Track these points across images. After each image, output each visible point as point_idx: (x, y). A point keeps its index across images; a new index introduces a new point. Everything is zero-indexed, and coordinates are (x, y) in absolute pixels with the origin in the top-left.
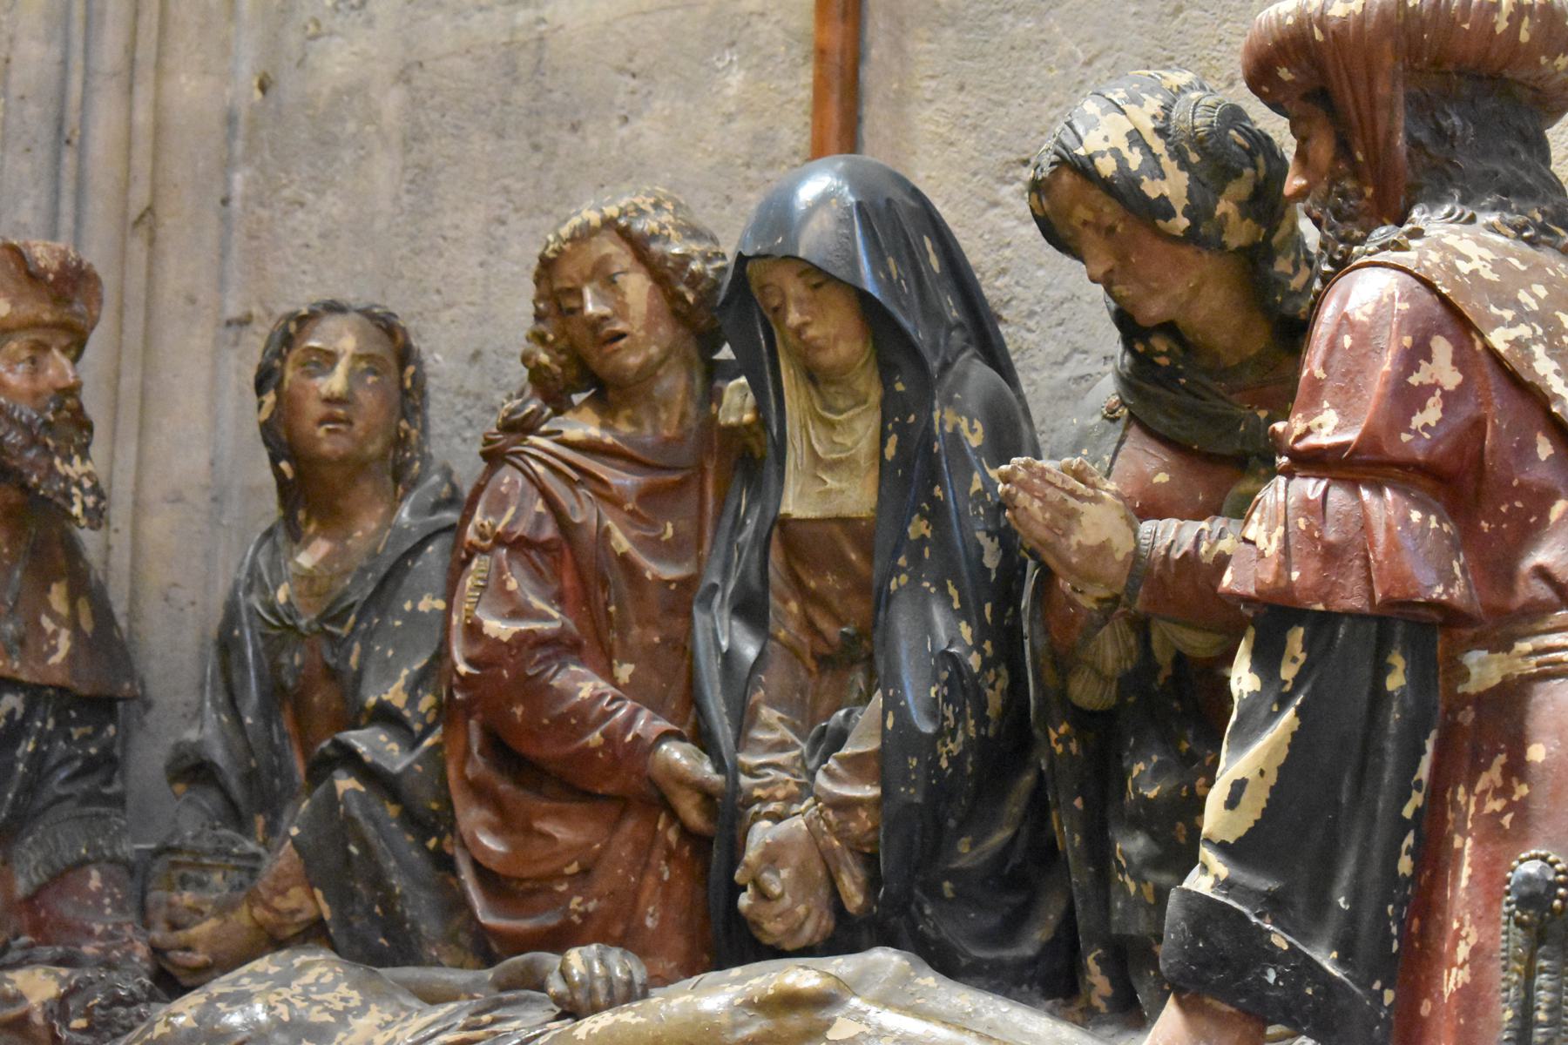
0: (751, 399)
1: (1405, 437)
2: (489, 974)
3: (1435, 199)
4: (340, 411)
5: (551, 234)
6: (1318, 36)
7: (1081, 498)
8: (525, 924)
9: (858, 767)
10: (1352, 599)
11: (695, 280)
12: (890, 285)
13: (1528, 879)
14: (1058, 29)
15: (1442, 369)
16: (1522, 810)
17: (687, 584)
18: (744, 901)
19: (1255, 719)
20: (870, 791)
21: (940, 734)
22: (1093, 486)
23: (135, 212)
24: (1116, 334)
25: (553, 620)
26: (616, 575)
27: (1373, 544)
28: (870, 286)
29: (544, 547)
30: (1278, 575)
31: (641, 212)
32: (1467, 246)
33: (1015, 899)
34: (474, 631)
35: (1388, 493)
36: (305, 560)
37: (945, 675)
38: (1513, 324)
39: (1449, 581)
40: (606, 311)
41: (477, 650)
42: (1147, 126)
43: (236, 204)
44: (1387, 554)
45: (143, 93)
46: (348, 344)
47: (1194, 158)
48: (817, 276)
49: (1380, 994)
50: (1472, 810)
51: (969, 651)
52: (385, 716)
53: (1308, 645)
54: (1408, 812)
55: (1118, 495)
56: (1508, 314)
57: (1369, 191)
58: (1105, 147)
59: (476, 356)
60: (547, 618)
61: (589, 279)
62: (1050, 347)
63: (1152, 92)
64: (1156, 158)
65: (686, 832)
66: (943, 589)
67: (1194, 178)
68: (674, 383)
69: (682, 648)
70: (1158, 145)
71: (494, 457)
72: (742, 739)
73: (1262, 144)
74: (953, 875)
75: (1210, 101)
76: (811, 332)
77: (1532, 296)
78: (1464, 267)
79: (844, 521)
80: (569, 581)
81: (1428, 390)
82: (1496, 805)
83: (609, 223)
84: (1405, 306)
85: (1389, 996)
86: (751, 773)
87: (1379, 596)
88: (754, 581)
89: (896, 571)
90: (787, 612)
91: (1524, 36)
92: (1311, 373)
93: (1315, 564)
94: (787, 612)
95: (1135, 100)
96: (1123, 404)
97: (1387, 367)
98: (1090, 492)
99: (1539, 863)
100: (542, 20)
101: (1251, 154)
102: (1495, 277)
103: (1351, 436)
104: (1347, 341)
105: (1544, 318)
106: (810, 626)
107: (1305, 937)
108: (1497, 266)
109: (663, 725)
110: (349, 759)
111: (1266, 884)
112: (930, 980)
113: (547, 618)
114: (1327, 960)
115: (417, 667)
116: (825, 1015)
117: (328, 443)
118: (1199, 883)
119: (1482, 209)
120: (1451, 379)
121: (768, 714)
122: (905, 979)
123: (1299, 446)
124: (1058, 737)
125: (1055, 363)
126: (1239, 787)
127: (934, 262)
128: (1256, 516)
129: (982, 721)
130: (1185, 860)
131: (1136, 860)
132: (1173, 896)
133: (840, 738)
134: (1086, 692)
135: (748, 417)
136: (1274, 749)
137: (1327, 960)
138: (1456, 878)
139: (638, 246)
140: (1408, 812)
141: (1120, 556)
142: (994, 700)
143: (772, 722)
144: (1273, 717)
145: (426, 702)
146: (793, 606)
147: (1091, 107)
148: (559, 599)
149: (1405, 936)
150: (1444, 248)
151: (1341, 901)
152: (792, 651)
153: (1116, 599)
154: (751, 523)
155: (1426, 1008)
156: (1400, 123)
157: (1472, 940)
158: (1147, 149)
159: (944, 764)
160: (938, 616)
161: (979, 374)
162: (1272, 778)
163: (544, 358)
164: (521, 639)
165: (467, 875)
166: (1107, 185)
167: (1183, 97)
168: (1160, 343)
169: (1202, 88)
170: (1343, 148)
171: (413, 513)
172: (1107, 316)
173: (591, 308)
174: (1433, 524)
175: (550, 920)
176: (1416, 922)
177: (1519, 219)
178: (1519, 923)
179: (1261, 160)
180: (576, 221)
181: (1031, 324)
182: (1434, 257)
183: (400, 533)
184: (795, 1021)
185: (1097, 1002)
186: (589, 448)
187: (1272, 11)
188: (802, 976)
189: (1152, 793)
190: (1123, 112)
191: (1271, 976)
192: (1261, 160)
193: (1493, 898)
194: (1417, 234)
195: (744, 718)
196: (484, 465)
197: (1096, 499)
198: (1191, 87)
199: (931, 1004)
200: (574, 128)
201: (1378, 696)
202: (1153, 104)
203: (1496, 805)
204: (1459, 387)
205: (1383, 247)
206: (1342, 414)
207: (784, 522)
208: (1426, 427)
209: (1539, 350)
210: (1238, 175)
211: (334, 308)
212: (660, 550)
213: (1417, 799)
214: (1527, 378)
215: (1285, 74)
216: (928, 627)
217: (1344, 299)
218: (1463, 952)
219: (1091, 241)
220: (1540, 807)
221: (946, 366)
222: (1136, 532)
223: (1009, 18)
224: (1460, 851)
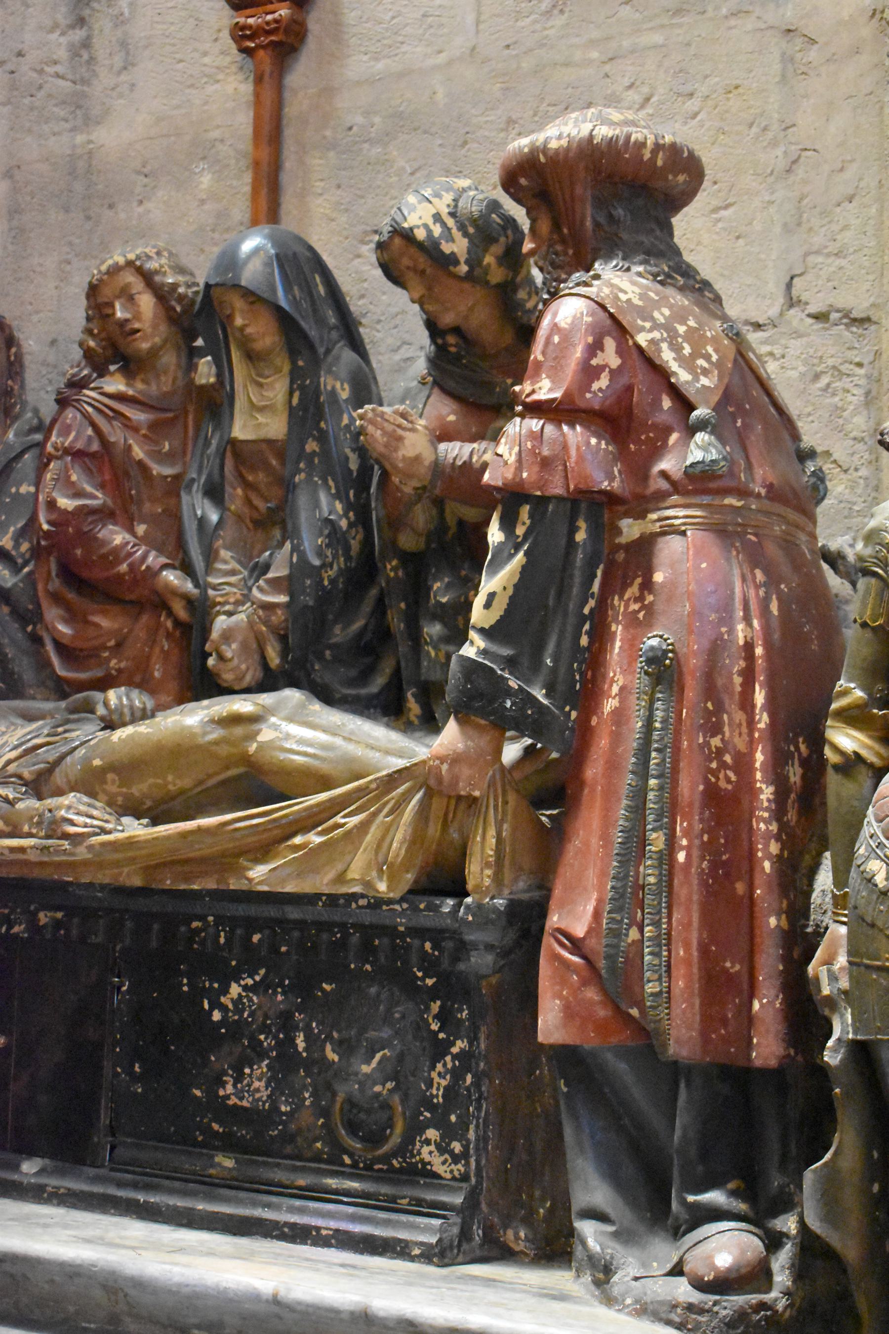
0: (214, 370)
1: (588, 395)
2: (63, 704)
3: (608, 257)
5: (95, 269)
6: (542, 159)
7: (404, 429)
8: (83, 676)
9: (276, 585)
10: (557, 490)
11: (181, 298)
12: (295, 302)
13: (652, 648)
14: (395, 153)
15: (610, 356)
16: (649, 610)
17: (177, 478)
18: (211, 662)
19: (502, 556)
20: (283, 599)
21: (323, 566)
22: (411, 422)
24: (426, 333)
25: (98, 498)
26: (134, 472)
27: (569, 458)
28: (283, 303)
29: (93, 456)
30: (515, 475)
31: (149, 258)
32: (625, 284)
33: (367, 660)
34: (51, 504)
35: (578, 428)
37: (326, 532)
38: (650, 330)
39: (612, 479)
40: (128, 316)
41: (53, 517)
42: (444, 211)
44: (577, 463)
47: (471, 230)
48: (250, 296)
49: (569, 713)
50: (622, 609)
51: (340, 517)
53: (531, 516)
54: (586, 611)
55: (426, 427)
56: (648, 325)
57: (571, 252)
58: (419, 223)
59: (53, 342)
60: (93, 497)
61: (118, 297)
62: (390, 341)
63: (447, 191)
64: (449, 229)
65: (177, 623)
66: (325, 482)
67: (471, 241)
68: (169, 359)
69: (175, 516)
70: (450, 222)
71: (63, 402)
72: (209, 569)
73: (510, 222)
74: (331, 647)
75: (481, 197)
76: (249, 330)
77: (661, 315)
78: (623, 297)
79: (269, 442)
80: (107, 477)
81: (601, 368)
82: (636, 607)
83: (130, 264)
84: (589, 319)
85: (574, 714)
86: (214, 588)
87: (572, 487)
88: (216, 476)
89: (299, 471)
90: (235, 495)
91: (660, 163)
92: (535, 358)
93: (536, 469)
94: (235, 495)
95: (438, 195)
96: (430, 374)
97: (578, 355)
98: (410, 426)
99: (658, 639)
100: (90, 142)
101: (504, 228)
102: (640, 303)
103: (558, 394)
104: (556, 339)
105: (668, 328)
106: (248, 502)
107: (528, 682)
108: (642, 296)
109: (163, 560)
111: (506, 652)
112: (317, 706)
113: (93, 497)
114: (539, 694)
115: (19, 525)
116: (256, 727)
118: (469, 651)
119: (635, 264)
120: (615, 362)
122: (303, 706)
123: (528, 400)
124: (391, 568)
125: (393, 351)
126: (492, 596)
127: (322, 290)
128: (503, 440)
129: (348, 558)
130: (461, 638)
131: (435, 638)
132: (454, 658)
133: (266, 568)
134: (407, 541)
135: (212, 380)
136: (512, 574)
137: (539, 694)
138: (613, 647)
139: (147, 278)
140: (586, 611)
141: (427, 463)
142: (355, 545)
144: (511, 556)
145: (25, 547)
146: (239, 491)
147: (412, 199)
148: (102, 486)
149: (583, 682)
150: (612, 285)
151: (548, 661)
152: (239, 518)
153: (424, 488)
154: (214, 443)
155: (594, 721)
156: (589, 211)
157: (620, 683)
158: (444, 224)
159: (326, 583)
160: (323, 498)
161: (348, 356)
162: (510, 591)
163: (92, 343)
164: (79, 509)
165: (50, 648)
166: (420, 245)
167: (465, 195)
168: (451, 339)
169: (477, 189)
170: (556, 226)
171: (16, 435)
172: (421, 323)
173: (119, 314)
174: (603, 446)
175: (99, 673)
176: (590, 673)
177: (655, 270)
178: (646, 673)
179: (509, 232)
180: (110, 262)
181: (379, 327)
182: (606, 291)
183: (8, 446)
184: (239, 731)
185: (413, 718)
186: (120, 397)
187: (516, 144)
188: (243, 705)
189: (444, 600)
190: (430, 202)
191: (508, 704)
192: (509, 232)
193: (632, 660)
194: (597, 277)
195: (210, 556)
196: (56, 407)
197: (413, 430)
198: (470, 188)
199: (317, 721)
200: (111, 206)
201: (571, 544)
202: (448, 198)
203: (636, 607)
204: (619, 367)
205: (578, 285)
206: (553, 382)
207: (234, 443)
208: (600, 390)
209: (664, 346)
210: (495, 240)
212: (163, 458)
213: (592, 603)
214: (658, 362)
215: (523, 181)
216: (317, 505)
217: (555, 315)
218: (615, 689)
219: (412, 279)
220: (659, 607)
221: (328, 351)
222: (436, 449)
223: (366, 146)
224: (615, 633)
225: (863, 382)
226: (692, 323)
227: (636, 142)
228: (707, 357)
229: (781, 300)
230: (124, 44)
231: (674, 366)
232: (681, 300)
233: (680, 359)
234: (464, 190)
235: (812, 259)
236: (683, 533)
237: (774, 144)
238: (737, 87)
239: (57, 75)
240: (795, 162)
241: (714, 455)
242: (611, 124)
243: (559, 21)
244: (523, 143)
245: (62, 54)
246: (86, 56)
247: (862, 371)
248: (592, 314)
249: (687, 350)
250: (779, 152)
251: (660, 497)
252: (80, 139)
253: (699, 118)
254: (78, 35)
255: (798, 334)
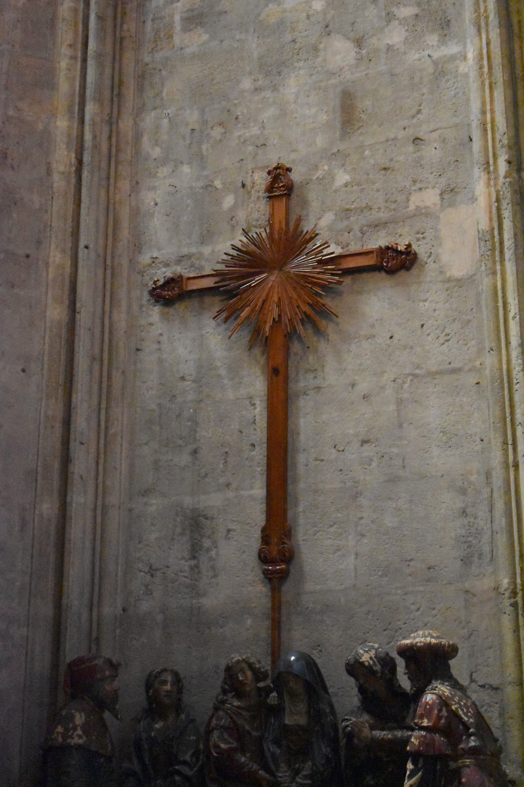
4: (170, 694)
9: (306, 777)
11: (262, 672)
15: (444, 713)
23: (93, 639)
25: (235, 745)
32: (445, 690)
34: (217, 746)
36: (157, 726)
38: (455, 705)
40: (244, 678)
42: (373, 656)
43: (117, 637)
45: (95, 610)
46: (169, 678)
48: (296, 676)
52: (185, 763)
58: (365, 660)
60: (233, 744)
61: (239, 672)
70: (375, 660)
71: (216, 709)
78: (446, 694)
79: (299, 726)
83: (244, 660)
86: (281, 777)
104: (428, 707)
108: (451, 693)
110: (179, 773)
115: (192, 752)
117: (167, 701)
121: (282, 765)
135: (276, 703)
136: (417, 779)
139: (251, 666)
143: (283, 767)
145: (194, 759)
158: (373, 661)
160: (323, 747)
164: (229, 748)
166: (366, 667)
186: (238, 707)
197: (366, 727)
202: (373, 652)
207: (285, 725)
209: (459, 709)
211: (165, 670)
214: (458, 714)
217: (426, 699)
222: (372, 733)
225: (498, 709)
226: (464, 701)
227: (443, 644)
228: (470, 712)
229: (469, 680)
230: (213, 568)
231: (463, 716)
232: (459, 693)
233: (464, 713)
234: (378, 648)
235: (478, 667)
236: (470, 767)
237: (464, 628)
238: (450, 608)
239: (184, 577)
240: (471, 634)
241: (478, 743)
242: (432, 637)
243: (386, 579)
244: (408, 642)
245: (187, 568)
246: (196, 571)
247: (497, 705)
248: (437, 699)
249: (465, 711)
250: (465, 630)
251: (462, 756)
252: (194, 601)
253: (437, 617)
254: (193, 562)
255: (476, 692)
